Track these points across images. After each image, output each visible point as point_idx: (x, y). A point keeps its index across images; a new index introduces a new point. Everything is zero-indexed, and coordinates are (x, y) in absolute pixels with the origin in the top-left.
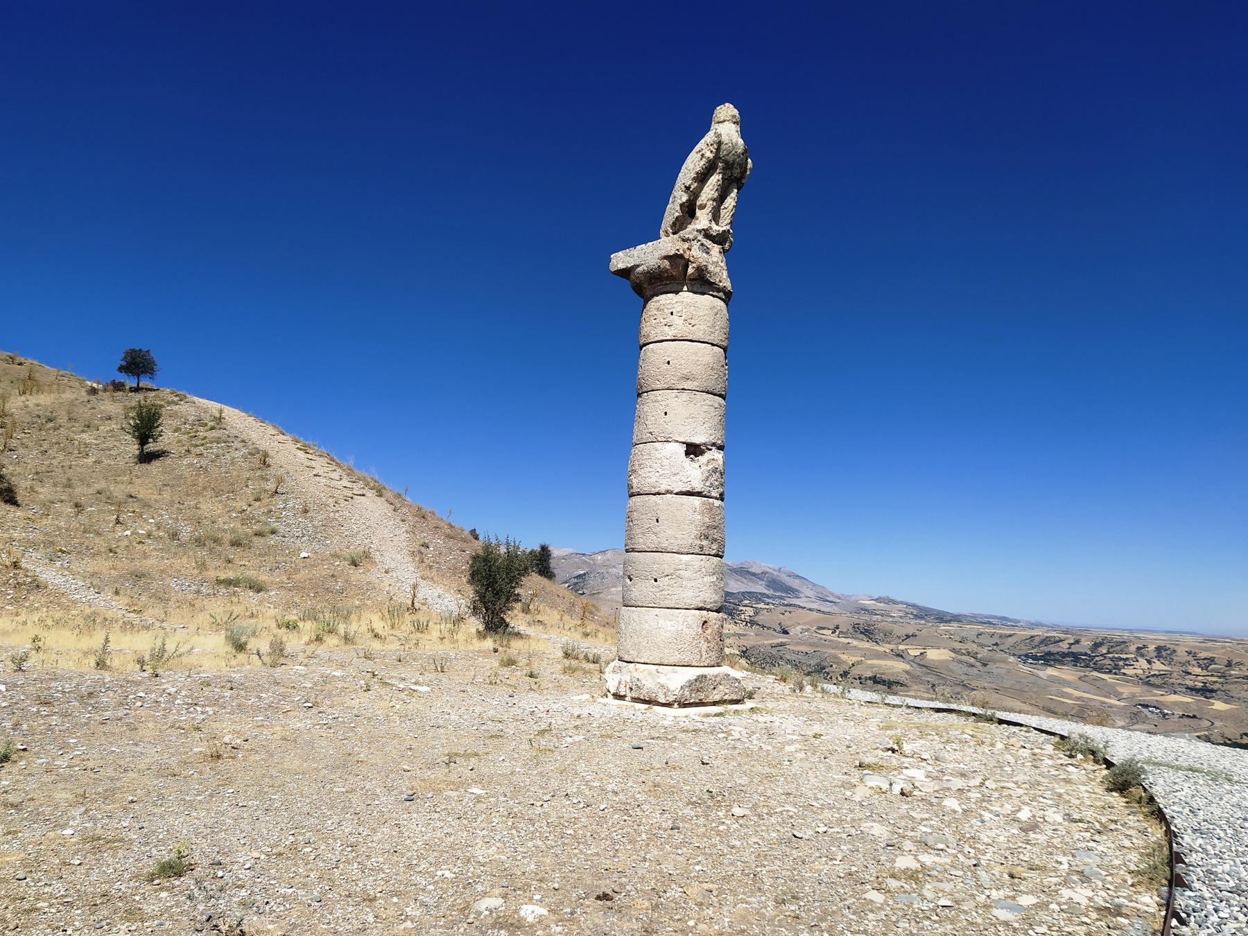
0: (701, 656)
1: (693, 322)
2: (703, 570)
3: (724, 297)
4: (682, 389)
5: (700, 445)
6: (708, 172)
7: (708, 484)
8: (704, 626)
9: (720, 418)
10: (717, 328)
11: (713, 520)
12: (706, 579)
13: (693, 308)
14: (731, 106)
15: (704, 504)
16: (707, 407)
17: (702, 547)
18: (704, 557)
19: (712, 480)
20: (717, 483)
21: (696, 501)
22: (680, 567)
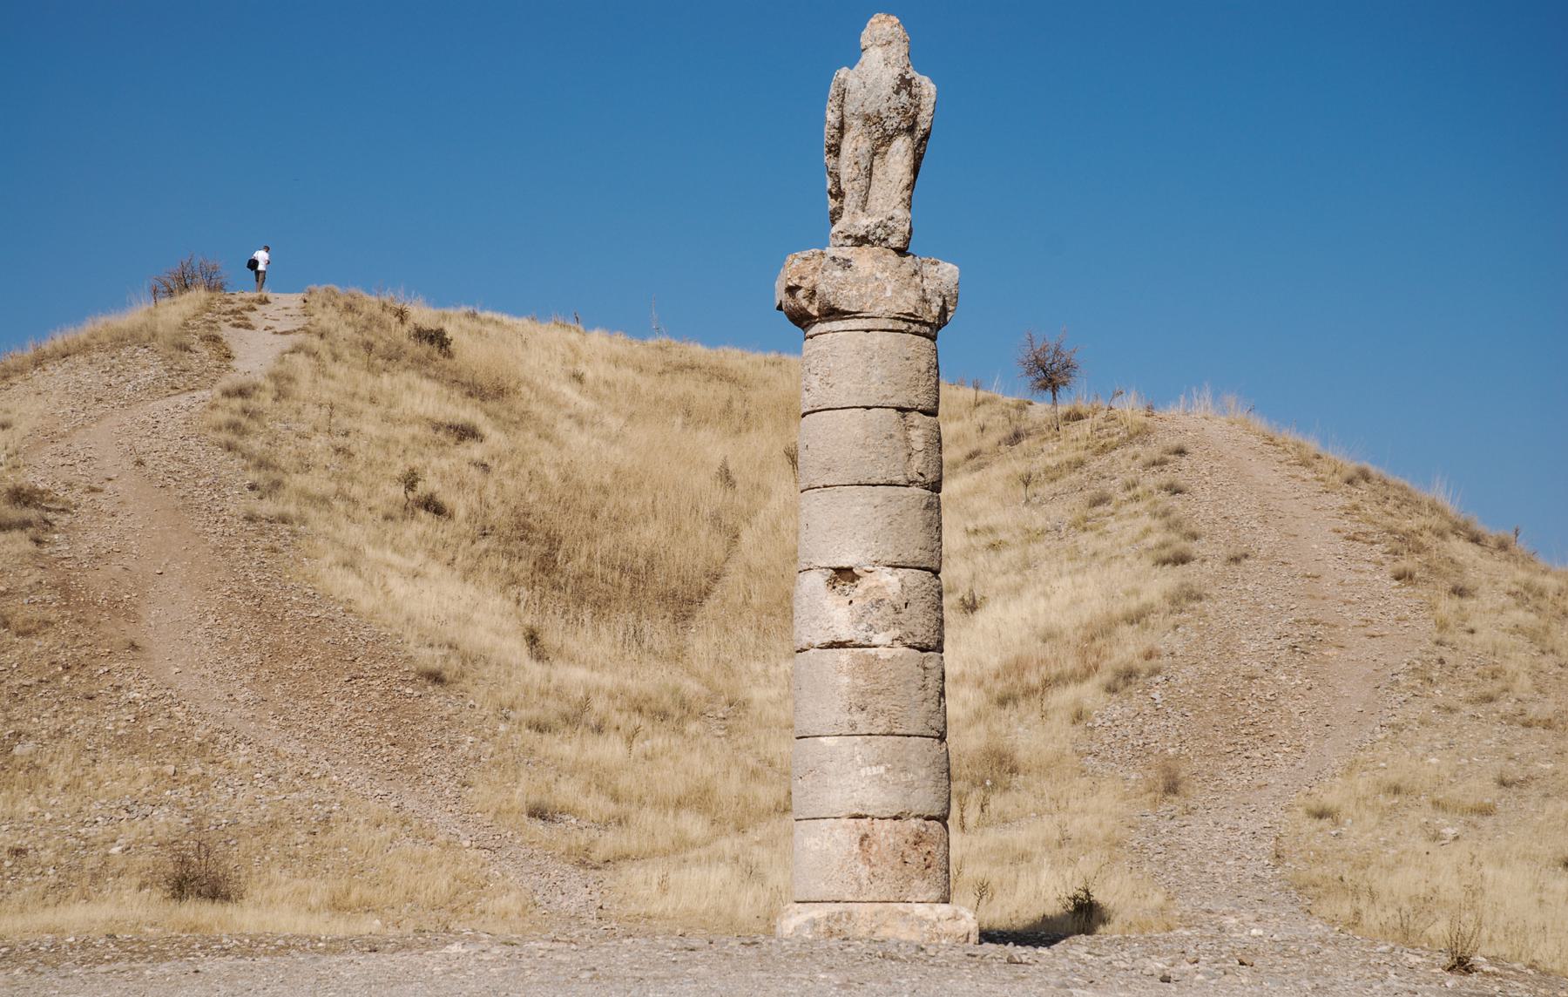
0: (860, 885)
1: (831, 380)
2: (858, 758)
3: (890, 327)
4: (825, 487)
5: (850, 569)
6: (842, 137)
7: (863, 626)
8: (866, 843)
9: (889, 520)
10: (873, 380)
11: (873, 681)
12: (863, 772)
13: (830, 358)
14: (883, 17)
15: (855, 658)
16: (858, 509)
17: (853, 725)
18: (859, 738)
19: (869, 619)
20: (880, 623)
21: (844, 655)
22: (823, 757)
